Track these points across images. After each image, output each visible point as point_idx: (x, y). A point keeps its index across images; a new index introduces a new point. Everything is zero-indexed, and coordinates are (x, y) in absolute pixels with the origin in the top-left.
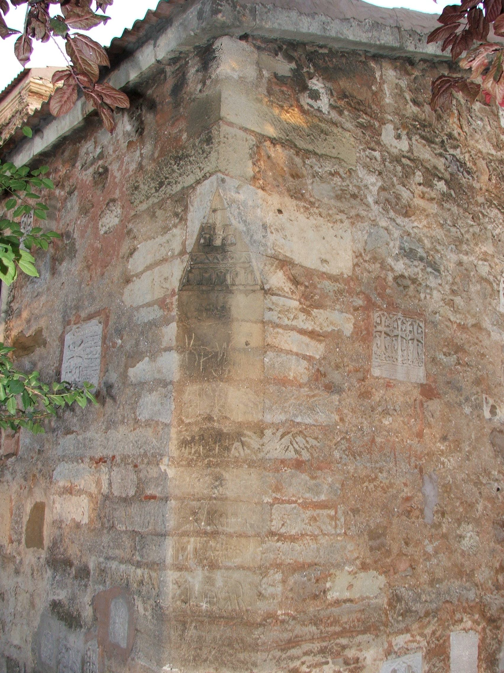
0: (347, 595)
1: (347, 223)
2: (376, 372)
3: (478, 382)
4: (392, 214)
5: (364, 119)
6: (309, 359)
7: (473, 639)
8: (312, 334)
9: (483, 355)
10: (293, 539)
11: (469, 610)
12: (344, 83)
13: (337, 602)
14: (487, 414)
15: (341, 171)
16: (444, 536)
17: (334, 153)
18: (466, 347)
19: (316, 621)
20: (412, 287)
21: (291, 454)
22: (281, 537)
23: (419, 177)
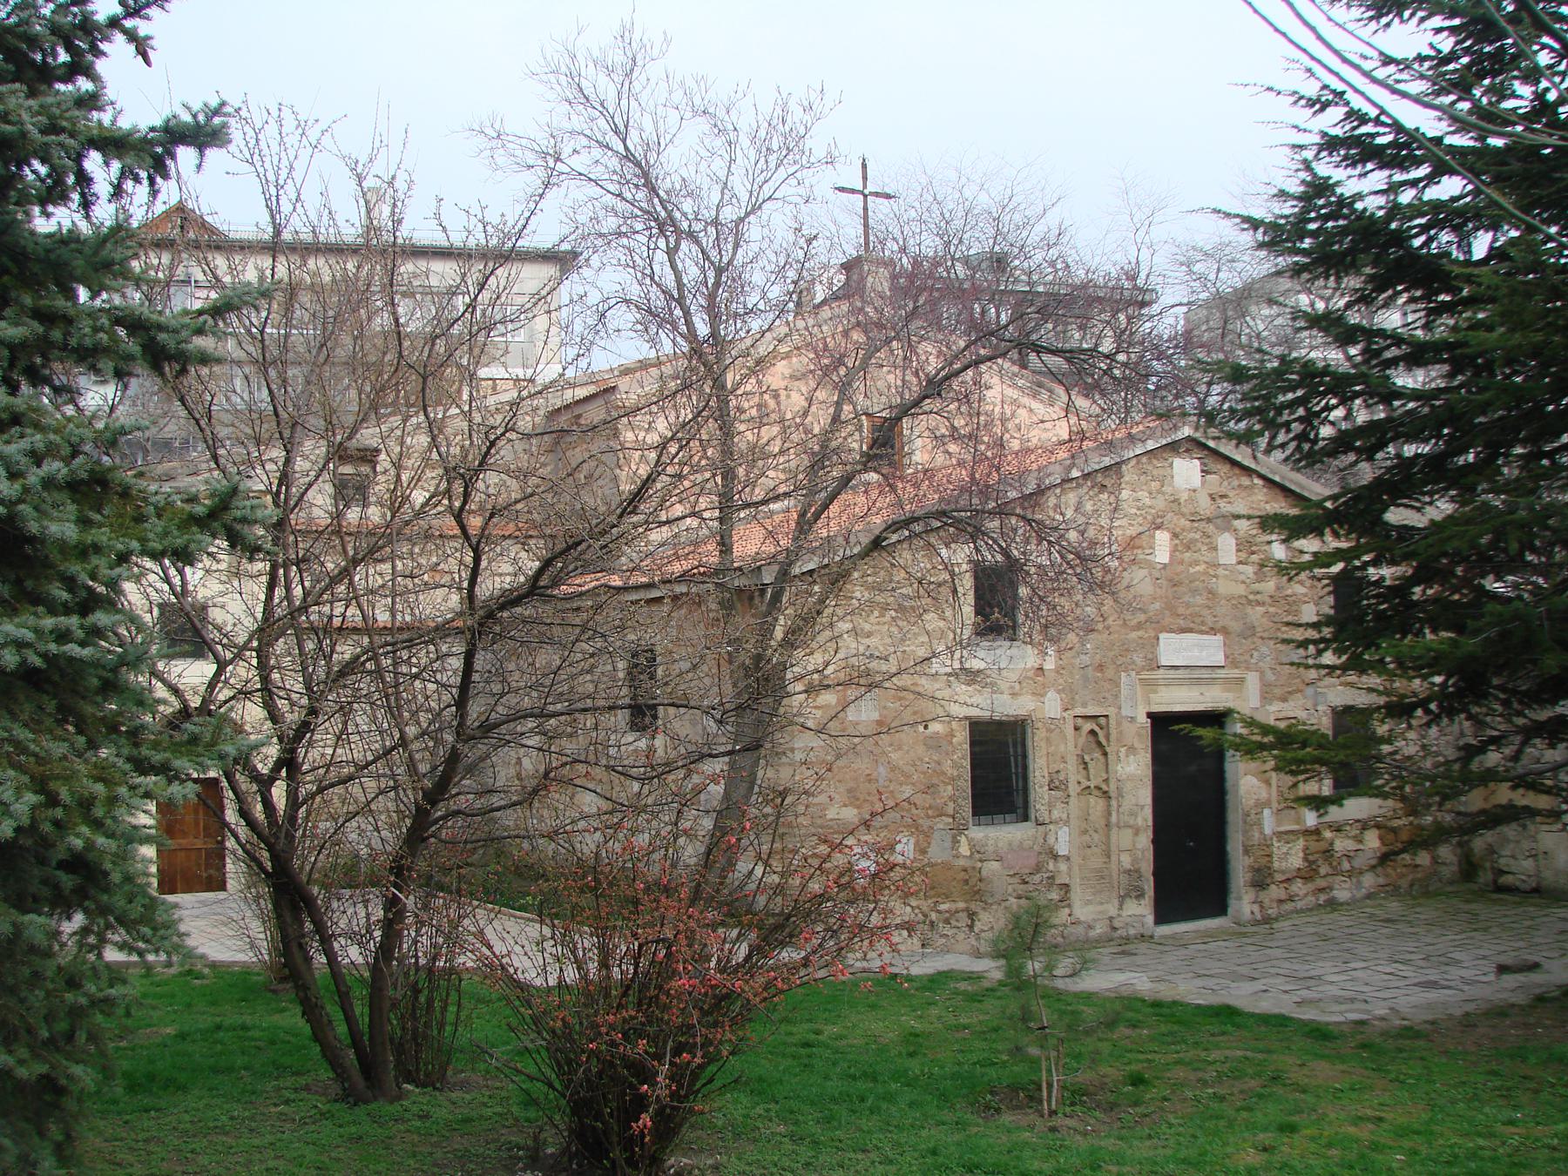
23: (876, 613)
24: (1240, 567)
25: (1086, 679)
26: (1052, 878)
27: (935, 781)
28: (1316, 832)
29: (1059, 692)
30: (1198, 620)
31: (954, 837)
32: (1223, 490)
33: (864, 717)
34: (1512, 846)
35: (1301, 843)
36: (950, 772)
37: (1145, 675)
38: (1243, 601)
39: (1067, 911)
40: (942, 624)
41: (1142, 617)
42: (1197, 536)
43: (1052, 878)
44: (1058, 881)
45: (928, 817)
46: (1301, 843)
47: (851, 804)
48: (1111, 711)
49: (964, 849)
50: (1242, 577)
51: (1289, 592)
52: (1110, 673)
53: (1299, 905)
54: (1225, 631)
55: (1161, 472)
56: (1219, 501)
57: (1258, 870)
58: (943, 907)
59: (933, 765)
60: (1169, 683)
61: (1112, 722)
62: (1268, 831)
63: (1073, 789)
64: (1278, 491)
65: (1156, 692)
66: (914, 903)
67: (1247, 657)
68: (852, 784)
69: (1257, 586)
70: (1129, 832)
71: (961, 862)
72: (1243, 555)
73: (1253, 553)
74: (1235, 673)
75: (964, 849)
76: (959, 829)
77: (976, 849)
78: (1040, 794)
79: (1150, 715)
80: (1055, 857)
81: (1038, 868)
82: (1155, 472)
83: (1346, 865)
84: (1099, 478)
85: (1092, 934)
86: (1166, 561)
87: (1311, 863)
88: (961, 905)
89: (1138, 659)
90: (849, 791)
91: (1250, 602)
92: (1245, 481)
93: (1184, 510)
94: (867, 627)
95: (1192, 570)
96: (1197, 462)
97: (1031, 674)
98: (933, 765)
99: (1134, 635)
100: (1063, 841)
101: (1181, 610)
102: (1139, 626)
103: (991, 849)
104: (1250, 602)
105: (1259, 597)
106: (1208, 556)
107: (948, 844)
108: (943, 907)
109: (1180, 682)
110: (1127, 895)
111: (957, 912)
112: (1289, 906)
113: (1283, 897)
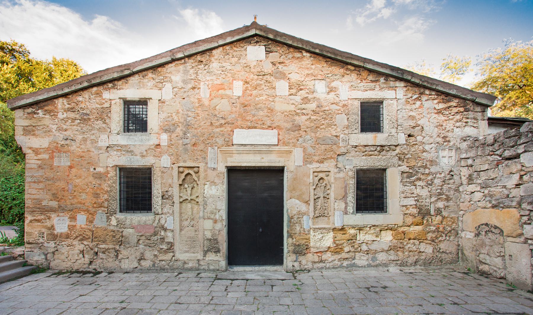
0: (47, 205)
1: (47, 137)
2: (55, 164)
3: (88, 163)
4: (61, 132)
5: (52, 114)
6: (37, 164)
7: (85, 217)
8: (38, 160)
9: (91, 157)
10: (34, 194)
11: (84, 211)
12: (46, 108)
13: (44, 206)
14: (92, 170)
15: (45, 127)
16: (75, 196)
17: (43, 124)
18: (85, 156)
19: (39, 208)
20: (66, 146)
21: (33, 180)
22: (30, 194)
23: (70, 121)
24: (292, 97)
25: (186, 150)
26: (163, 239)
27: (98, 192)
28: (342, 229)
29: (169, 156)
30: (260, 122)
31: (108, 217)
32: (281, 60)
33: (62, 164)
34: (487, 248)
35: (331, 234)
36: (106, 189)
37: (224, 148)
38: (294, 113)
39: (172, 254)
40: (104, 125)
41: (223, 122)
42: (262, 82)
43: (163, 239)
44: (166, 240)
45: (94, 207)
46: (331, 234)
47: (55, 200)
48: (201, 165)
49: (114, 222)
50: (292, 102)
51: (327, 108)
52: (201, 147)
53: (328, 266)
54: (278, 128)
55: (238, 53)
56: (278, 65)
57: (299, 245)
58: (101, 246)
59: (97, 185)
60: (239, 153)
61: (201, 170)
62: (305, 226)
63: (176, 200)
64: (321, 58)
65: (231, 157)
66: (85, 243)
67: (295, 141)
68: (55, 192)
69: (303, 106)
70: (211, 221)
71: (112, 228)
72: (293, 91)
73: (301, 90)
74: (286, 148)
75: (114, 222)
76: (110, 214)
77: (120, 223)
78: (157, 201)
79: (227, 167)
80: (165, 230)
81: (155, 234)
82: (235, 54)
83: (364, 247)
84: (199, 58)
85: (186, 266)
86: (240, 94)
87: (337, 245)
88: (111, 246)
89: (220, 141)
90: (53, 194)
91: (297, 114)
92: (298, 55)
93: (252, 70)
94: (65, 127)
95: (257, 99)
96: (264, 47)
97: (152, 147)
98: (97, 185)
99: (218, 130)
100: (170, 222)
101: (248, 118)
102: (221, 125)
103: (128, 222)
104: (297, 114)
105: (304, 111)
106: (270, 92)
107: (105, 219)
108: (101, 246)
109: (248, 152)
110: (208, 251)
111: (108, 249)
112: (321, 265)
113: (317, 260)
